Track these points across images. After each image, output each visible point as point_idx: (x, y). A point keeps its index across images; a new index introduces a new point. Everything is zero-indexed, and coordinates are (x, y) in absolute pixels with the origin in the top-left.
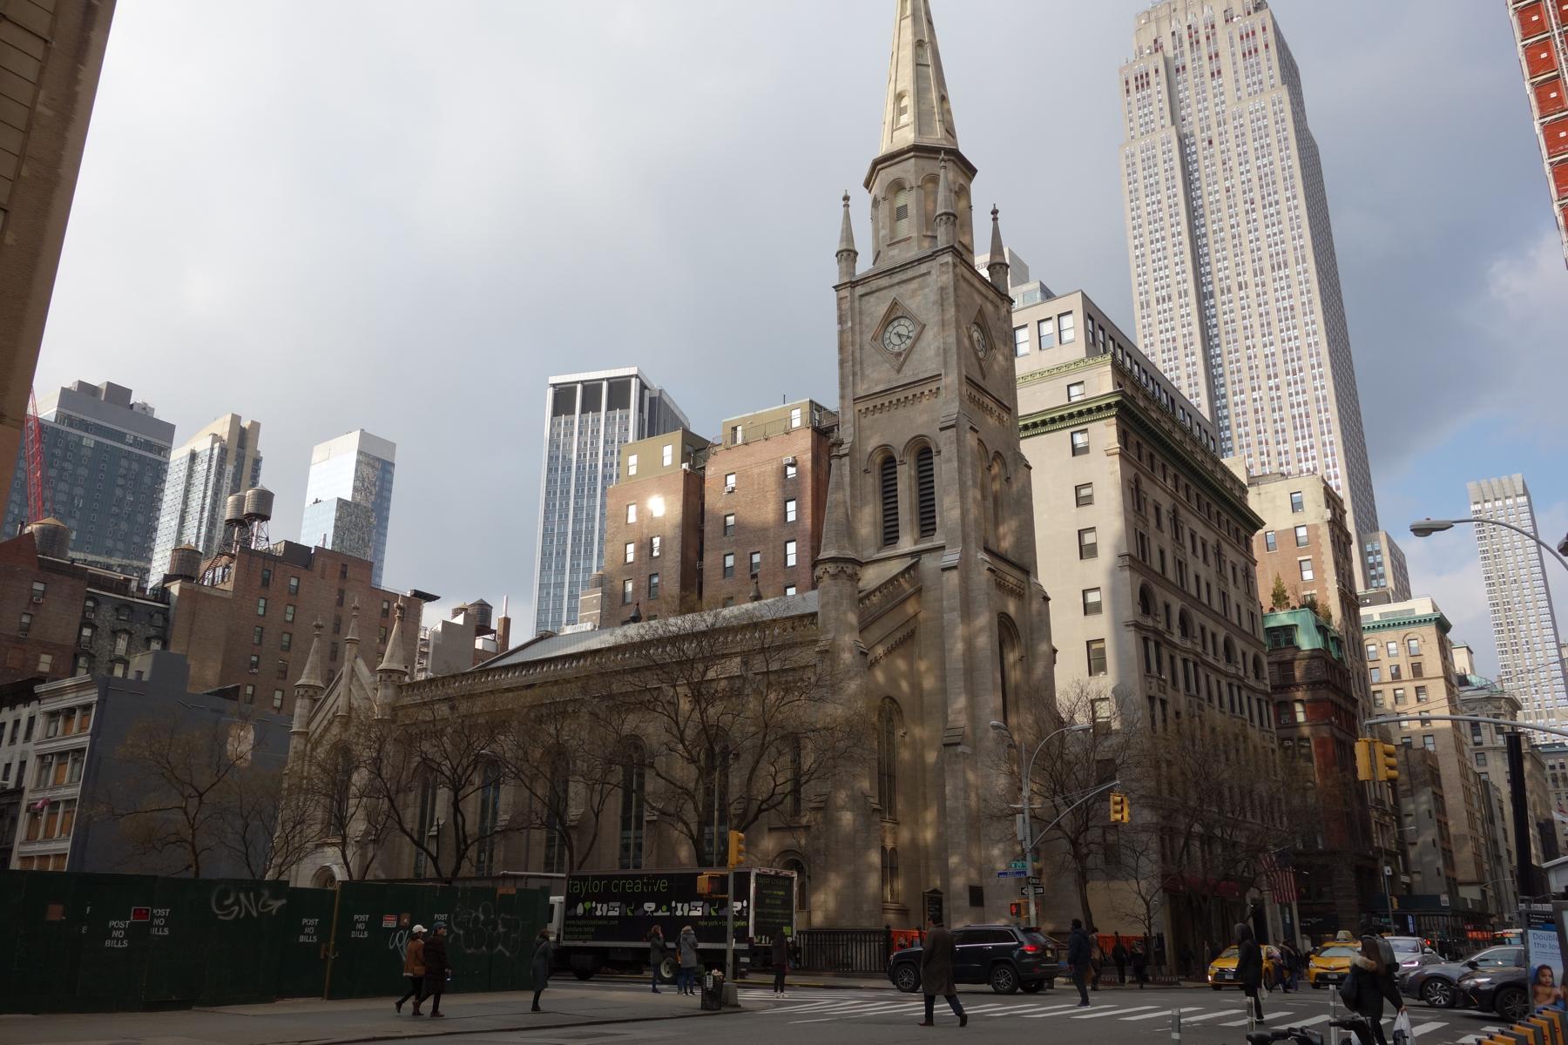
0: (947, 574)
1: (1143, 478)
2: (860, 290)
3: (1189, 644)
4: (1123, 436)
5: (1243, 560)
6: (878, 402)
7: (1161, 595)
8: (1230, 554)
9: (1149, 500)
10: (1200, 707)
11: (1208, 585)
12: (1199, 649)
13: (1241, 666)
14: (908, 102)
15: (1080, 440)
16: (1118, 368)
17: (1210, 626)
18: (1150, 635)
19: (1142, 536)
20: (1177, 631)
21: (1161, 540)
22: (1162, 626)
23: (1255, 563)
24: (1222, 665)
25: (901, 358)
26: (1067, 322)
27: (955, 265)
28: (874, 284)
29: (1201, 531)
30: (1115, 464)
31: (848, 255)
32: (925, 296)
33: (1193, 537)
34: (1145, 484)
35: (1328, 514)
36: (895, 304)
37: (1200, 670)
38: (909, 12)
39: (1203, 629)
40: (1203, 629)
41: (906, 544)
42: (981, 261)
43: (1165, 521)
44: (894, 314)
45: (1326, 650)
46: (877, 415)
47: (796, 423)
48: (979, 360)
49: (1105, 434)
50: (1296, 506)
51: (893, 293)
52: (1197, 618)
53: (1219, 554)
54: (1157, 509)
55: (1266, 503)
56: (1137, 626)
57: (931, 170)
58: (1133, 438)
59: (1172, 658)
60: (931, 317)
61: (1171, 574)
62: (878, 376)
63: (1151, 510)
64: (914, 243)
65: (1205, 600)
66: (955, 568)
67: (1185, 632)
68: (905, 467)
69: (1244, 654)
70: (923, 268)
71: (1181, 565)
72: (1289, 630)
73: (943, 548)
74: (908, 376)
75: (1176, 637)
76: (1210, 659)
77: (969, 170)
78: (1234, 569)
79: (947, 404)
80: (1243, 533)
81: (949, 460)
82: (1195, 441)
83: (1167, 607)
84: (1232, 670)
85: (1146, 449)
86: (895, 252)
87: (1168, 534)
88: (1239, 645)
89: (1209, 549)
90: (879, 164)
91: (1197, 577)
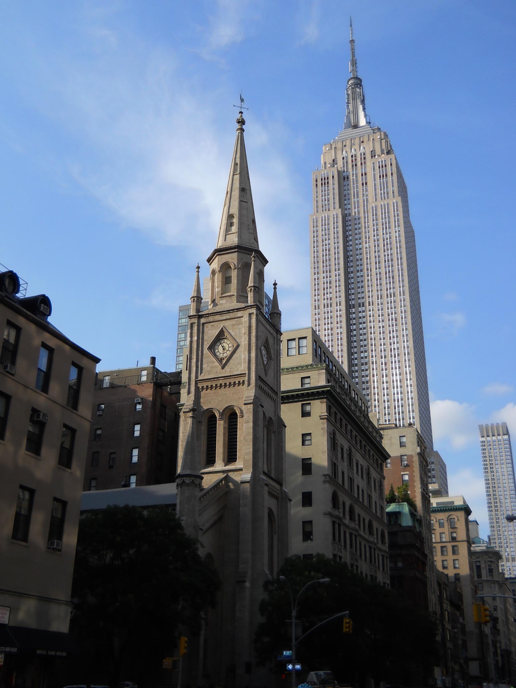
0: (243, 484)
1: (337, 432)
2: (203, 320)
3: (352, 525)
4: (329, 409)
5: (379, 476)
6: (209, 384)
7: (342, 497)
8: (374, 474)
9: (339, 444)
10: (357, 561)
11: (363, 491)
12: (357, 527)
13: (375, 536)
14: (235, 220)
15: (308, 408)
16: (330, 374)
17: (363, 514)
18: (335, 519)
19: (335, 464)
20: (347, 517)
21: (343, 466)
22: (341, 515)
23: (384, 478)
24: (367, 536)
25: (224, 363)
26: (304, 342)
28: (211, 319)
29: (362, 462)
30: (324, 424)
31: (198, 299)
32: (242, 329)
33: (357, 464)
34: (338, 436)
35: (418, 450)
37: (376, 551)
38: (238, 172)
39: (359, 516)
40: (359, 516)
41: (219, 465)
43: (345, 455)
44: (220, 337)
45: (414, 526)
46: (209, 390)
47: (144, 379)
48: (265, 366)
49: (319, 408)
50: (402, 445)
51: (221, 325)
52: (357, 510)
53: (368, 474)
54: (342, 449)
55: (390, 444)
56: (330, 514)
58: (333, 409)
59: (345, 532)
60: (244, 342)
61: (346, 485)
62: (211, 368)
63: (339, 450)
64: (235, 298)
65: (361, 500)
66: (248, 482)
67: (352, 518)
69: (377, 530)
70: (239, 314)
71: (351, 480)
72: (396, 515)
73: (241, 470)
74: (227, 371)
75: (347, 521)
76: (362, 533)
77: (265, 261)
78: (375, 481)
79: (249, 392)
80: (380, 461)
81: (247, 422)
82: (356, 404)
83: (344, 504)
84: (371, 539)
85: (339, 416)
86: (223, 301)
87: (346, 464)
88: (375, 524)
89: (364, 470)
91: (358, 487)
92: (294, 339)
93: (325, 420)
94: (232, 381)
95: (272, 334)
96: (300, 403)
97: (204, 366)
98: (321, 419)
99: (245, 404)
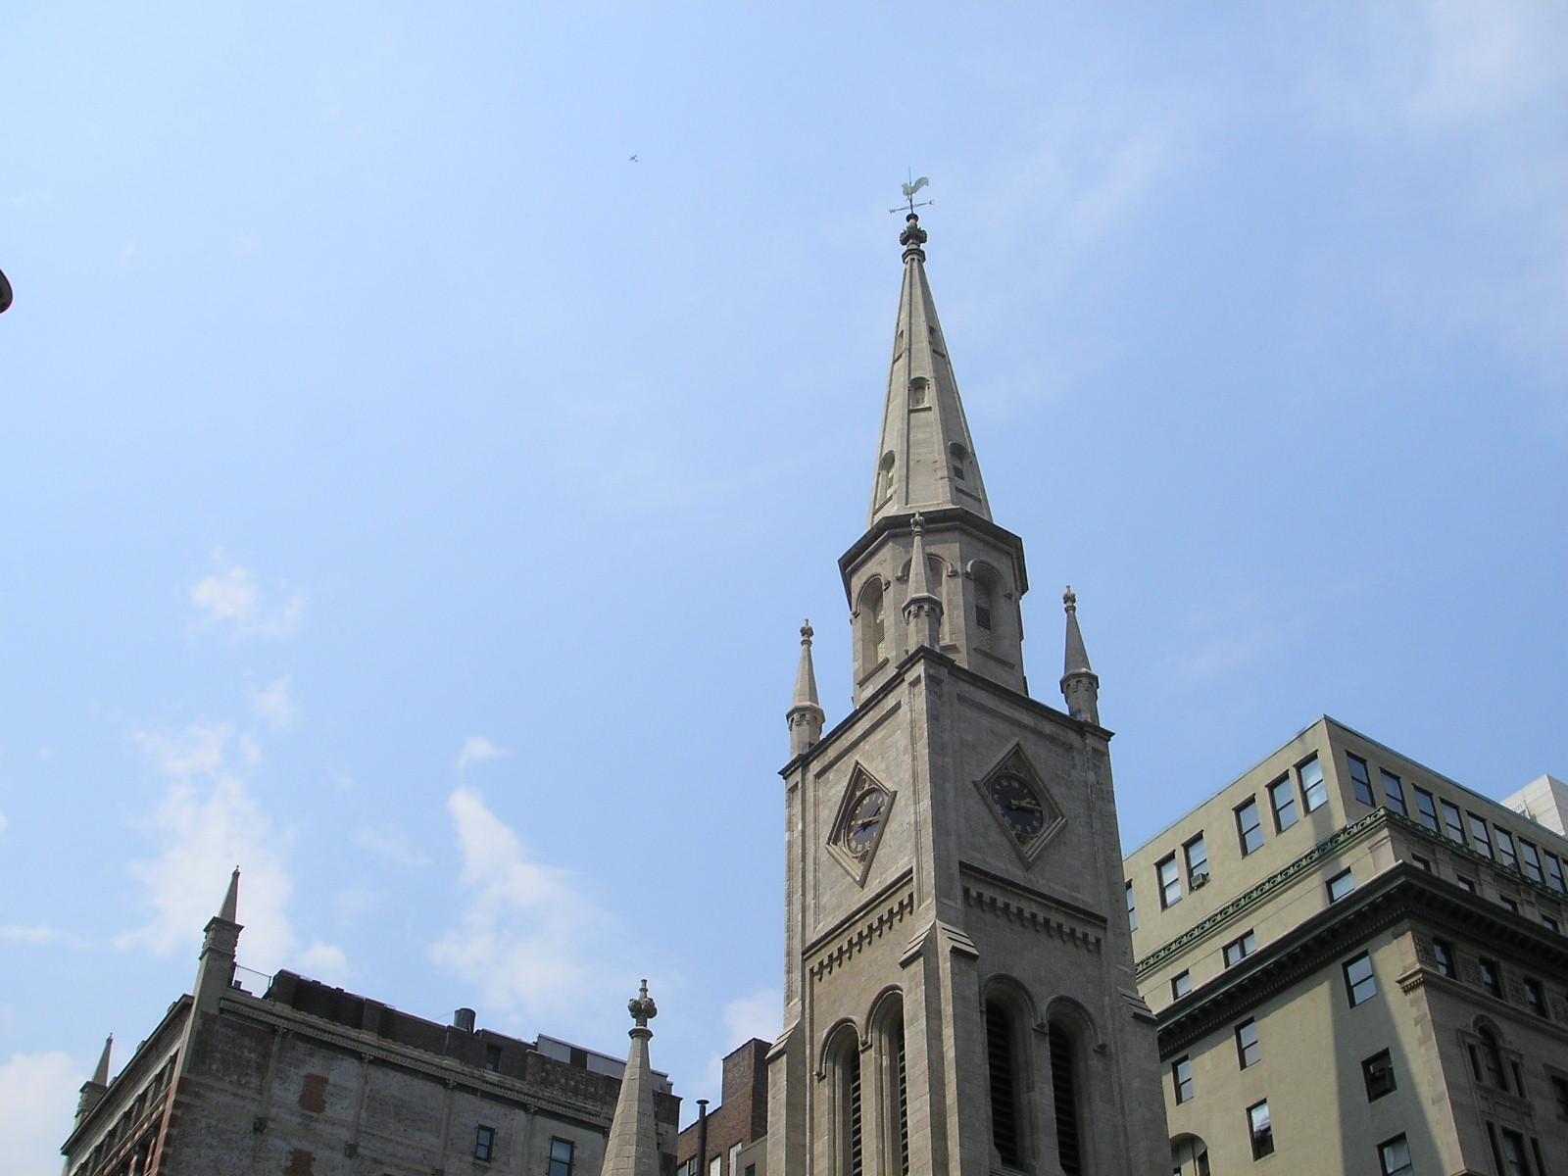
6: (833, 948)
19: (1515, 1138)
26: (1312, 775)
27: (932, 680)
34: (1511, 1036)
36: (859, 775)
42: (1045, 686)
49: (1396, 956)
57: (948, 558)
58: (1465, 952)
68: (872, 1052)
70: (890, 701)
77: (1009, 545)
90: (850, 563)
92: (1285, 777)
93: (1421, 990)
94: (883, 911)
95: (1052, 739)
96: (1338, 965)
97: (825, 899)
98: (1406, 991)
99: (905, 964)
